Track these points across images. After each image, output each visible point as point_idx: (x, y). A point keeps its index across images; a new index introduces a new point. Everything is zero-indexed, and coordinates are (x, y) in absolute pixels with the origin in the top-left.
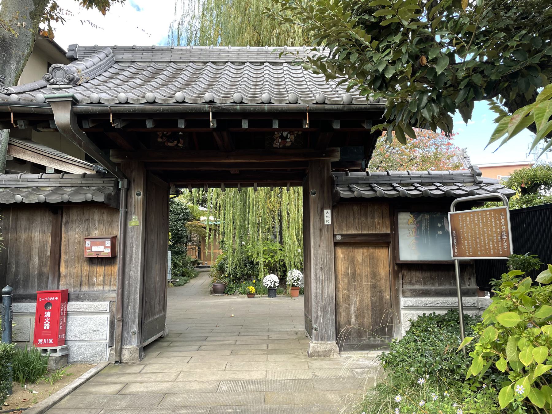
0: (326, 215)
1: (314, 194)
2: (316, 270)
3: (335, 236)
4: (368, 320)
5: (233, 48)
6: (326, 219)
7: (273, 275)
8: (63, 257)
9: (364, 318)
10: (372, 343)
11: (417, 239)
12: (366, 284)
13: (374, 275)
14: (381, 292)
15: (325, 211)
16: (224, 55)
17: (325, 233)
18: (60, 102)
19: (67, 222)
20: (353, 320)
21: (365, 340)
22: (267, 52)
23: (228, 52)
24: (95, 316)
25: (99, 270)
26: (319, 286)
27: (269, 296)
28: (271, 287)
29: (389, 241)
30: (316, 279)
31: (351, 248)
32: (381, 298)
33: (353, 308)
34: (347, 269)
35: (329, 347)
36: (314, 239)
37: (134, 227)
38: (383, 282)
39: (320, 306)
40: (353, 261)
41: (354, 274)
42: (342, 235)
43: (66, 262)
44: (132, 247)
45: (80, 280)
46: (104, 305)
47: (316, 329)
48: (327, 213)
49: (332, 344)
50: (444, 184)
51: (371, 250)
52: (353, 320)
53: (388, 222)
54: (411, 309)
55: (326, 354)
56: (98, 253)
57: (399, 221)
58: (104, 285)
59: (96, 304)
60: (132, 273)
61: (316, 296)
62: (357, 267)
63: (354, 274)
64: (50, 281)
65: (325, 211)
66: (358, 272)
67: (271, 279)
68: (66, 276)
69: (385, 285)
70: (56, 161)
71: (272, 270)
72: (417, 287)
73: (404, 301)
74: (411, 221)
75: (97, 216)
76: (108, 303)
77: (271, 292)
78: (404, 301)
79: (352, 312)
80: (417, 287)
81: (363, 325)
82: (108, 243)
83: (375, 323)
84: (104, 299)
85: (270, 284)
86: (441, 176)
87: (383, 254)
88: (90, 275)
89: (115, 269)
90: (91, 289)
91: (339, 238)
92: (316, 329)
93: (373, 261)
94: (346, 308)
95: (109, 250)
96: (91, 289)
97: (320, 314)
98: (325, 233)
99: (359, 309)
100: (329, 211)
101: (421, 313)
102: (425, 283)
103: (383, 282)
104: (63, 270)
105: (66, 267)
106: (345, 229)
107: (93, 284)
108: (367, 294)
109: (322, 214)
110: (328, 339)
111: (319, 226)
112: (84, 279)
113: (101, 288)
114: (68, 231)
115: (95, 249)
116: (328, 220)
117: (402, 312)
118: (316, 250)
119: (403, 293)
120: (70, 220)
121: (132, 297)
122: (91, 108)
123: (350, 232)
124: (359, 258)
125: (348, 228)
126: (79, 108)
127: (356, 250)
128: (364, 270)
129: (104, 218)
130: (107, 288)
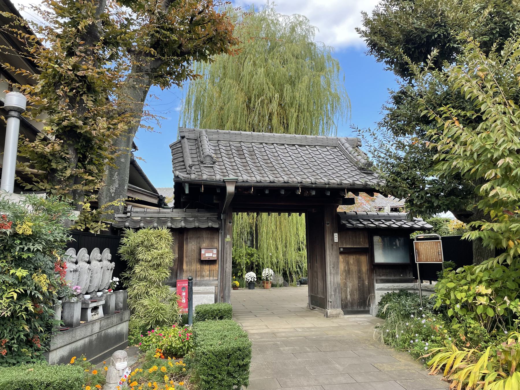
0: (335, 236)
1: (328, 224)
2: (330, 268)
3: (340, 248)
4: (356, 297)
5: (276, 134)
6: (335, 239)
7: (252, 272)
8: (185, 259)
9: (354, 295)
10: (359, 310)
11: (383, 251)
12: (355, 276)
13: (360, 271)
14: (363, 281)
15: (335, 234)
16: (271, 139)
17: (335, 247)
18: (231, 182)
19: (187, 238)
20: (349, 297)
21: (355, 308)
22: (296, 139)
23: (274, 137)
24: (206, 295)
25: (206, 267)
26: (332, 277)
27: (249, 289)
28: (251, 281)
29: (369, 252)
30: (330, 273)
31: (347, 255)
32: (363, 284)
33: (348, 289)
34: (345, 267)
35: (338, 312)
36: (329, 250)
37: (228, 242)
38: (364, 275)
39: (333, 289)
40: (348, 263)
41: (349, 271)
42: (343, 248)
43: (187, 262)
44: (227, 254)
45: (196, 273)
46: (212, 289)
47: (331, 302)
48: (336, 235)
49: (340, 310)
50: (397, 221)
51: (358, 256)
52: (349, 297)
53: (367, 241)
54: (381, 289)
55: (337, 316)
56: (209, 257)
57: (374, 241)
58: (210, 276)
59: (207, 288)
60: (227, 270)
61: (331, 283)
62: (350, 267)
63: (349, 271)
64: (178, 274)
65: (335, 234)
66: (351, 269)
67: (251, 276)
68: (187, 272)
69: (365, 277)
70: (132, 192)
71: (250, 268)
72: (383, 278)
73: (377, 286)
74: (380, 241)
75: (205, 234)
76: (214, 287)
77: (250, 285)
78: (377, 286)
79: (348, 292)
80: (383, 278)
81: (354, 300)
82: (215, 251)
83: (360, 298)
84: (211, 285)
85: (251, 279)
86: (395, 216)
87: (364, 259)
88: (201, 271)
89: (216, 267)
90: (202, 279)
91: (342, 250)
92: (331, 302)
93: (359, 263)
94: (345, 290)
95: (215, 256)
96: (202, 279)
97: (333, 293)
98: (335, 247)
99: (351, 291)
100: (337, 234)
101: (386, 292)
102: (387, 275)
103: (364, 275)
104: (185, 267)
105: (187, 266)
106: (344, 244)
107: (203, 276)
108: (356, 282)
109: (333, 236)
110: (337, 308)
111: (331, 243)
112: (198, 273)
113: (208, 278)
114: (187, 244)
115: (207, 255)
116: (336, 240)
117: (376, 292)
118: (330, 256)
119: (376, 281)
120: (189, 237)
121: (227, 284)
122: (243, 184)
123: (347, 247)
124: (351, 261)
125: (346, 244)
126: (238, 184)
127: (350, 257)
128: (354, 268)
129: (209, 236)
130: (211, 278)
